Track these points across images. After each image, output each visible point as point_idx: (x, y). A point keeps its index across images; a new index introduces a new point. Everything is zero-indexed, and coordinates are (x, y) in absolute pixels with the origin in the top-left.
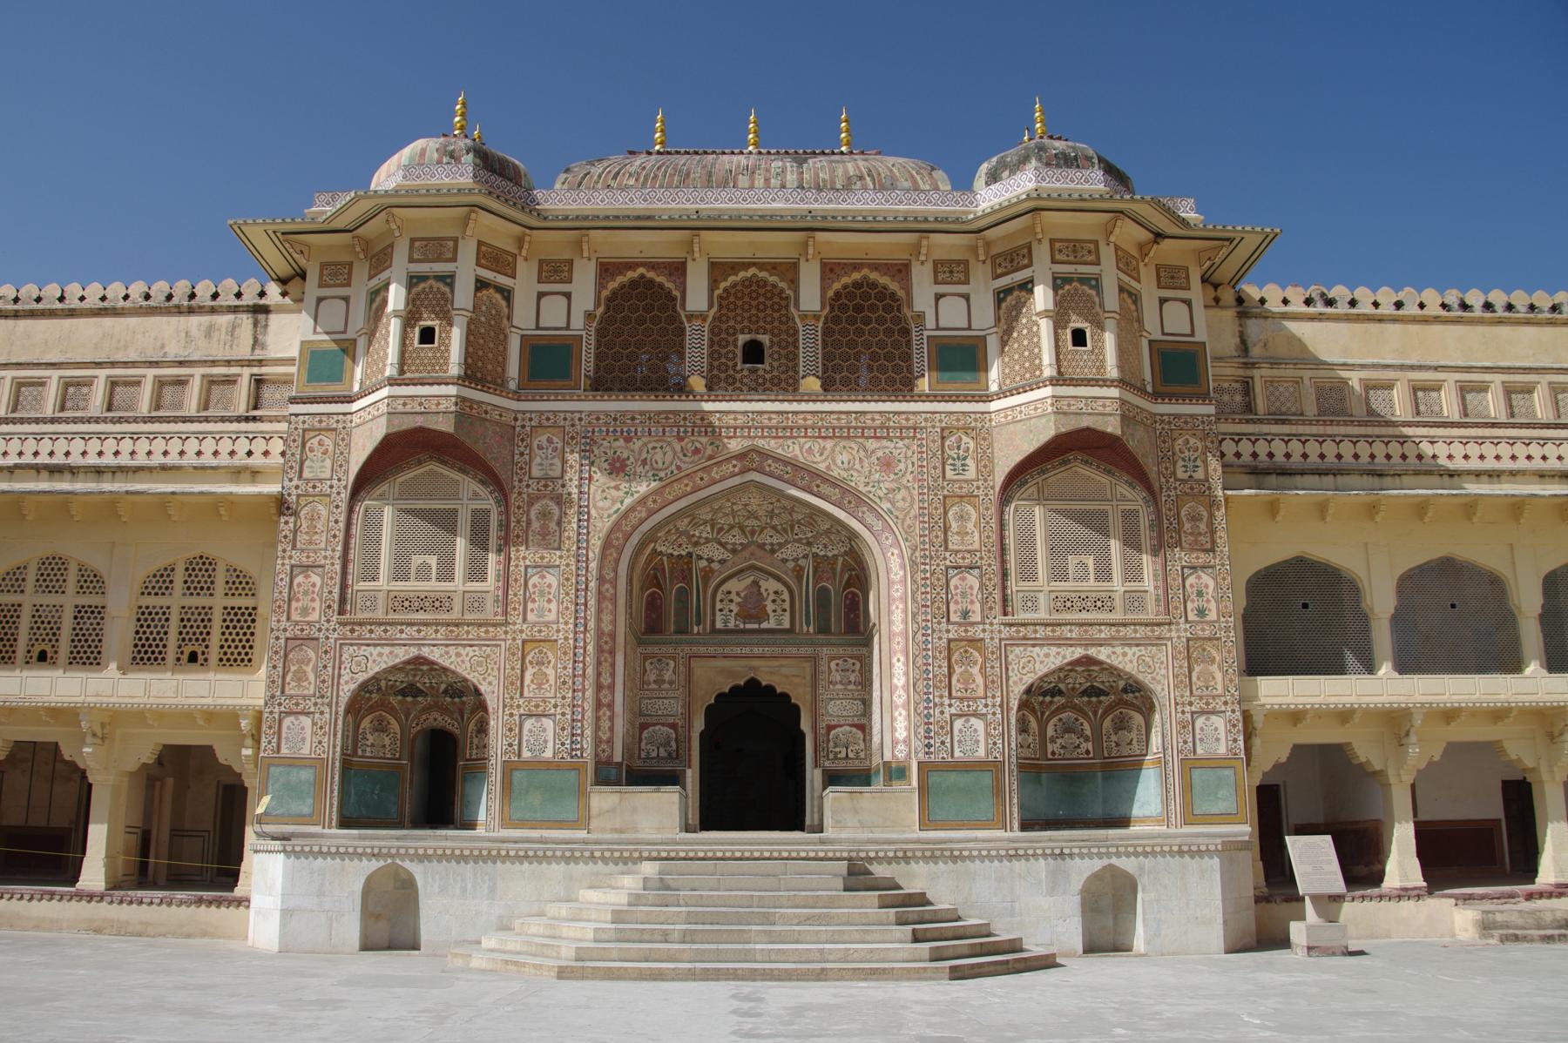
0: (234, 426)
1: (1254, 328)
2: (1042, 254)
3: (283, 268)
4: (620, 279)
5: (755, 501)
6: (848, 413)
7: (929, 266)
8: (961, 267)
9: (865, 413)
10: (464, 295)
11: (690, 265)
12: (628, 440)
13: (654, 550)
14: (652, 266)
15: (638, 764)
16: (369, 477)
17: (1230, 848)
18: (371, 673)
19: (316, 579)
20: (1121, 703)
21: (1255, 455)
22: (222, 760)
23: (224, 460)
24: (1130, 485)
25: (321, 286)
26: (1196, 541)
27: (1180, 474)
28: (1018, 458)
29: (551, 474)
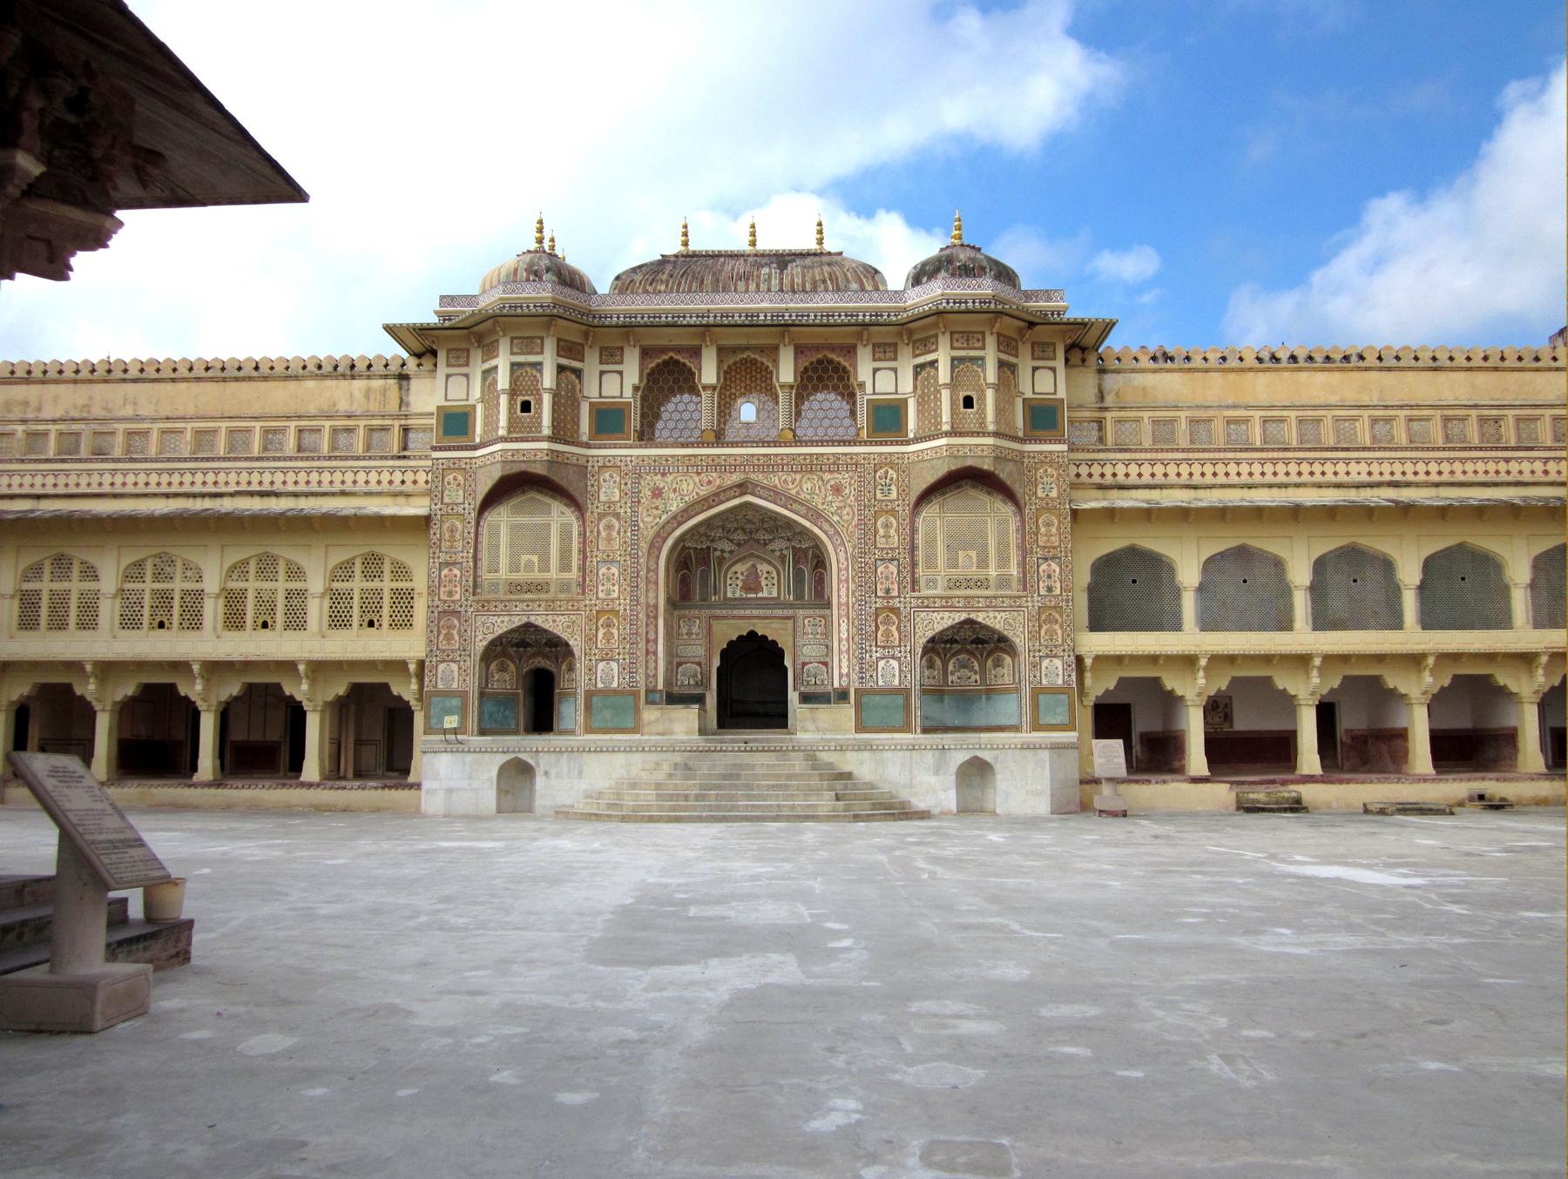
0: (391, 463)
1: (1110, 381)
3: (418, 348)
7: (870, 348)
12: (664, 475)
14: (679, 350)
15: (676, 690)
19: (456, 572)
21: (1102, 475)
23: (385, 486)
27: (1040, 494)
28: (924, 486)
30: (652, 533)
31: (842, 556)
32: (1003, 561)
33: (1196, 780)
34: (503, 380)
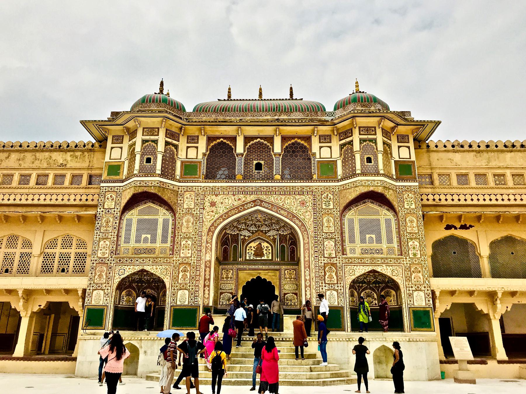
2: (356, 132)
5: (259, 216)
6: (290, 187)
7: (318, 137)
8: (329, 137)
9: (295, 186)
11: (238, 138)
12: (216, 195)
13: (225, 232)
14: (225, 138)
15: (219, 307)
20: (387, 287)
21: (434, 200)
22: (71, 307)
24: (388, 210)
25: (112, 143)
26: (412, 229)
27: (406, 206)
28: (348, 201)
29: (191, 207)
30: (210, 224)
32: (390, 240)
33: (500, 362)
34: (138, 148)
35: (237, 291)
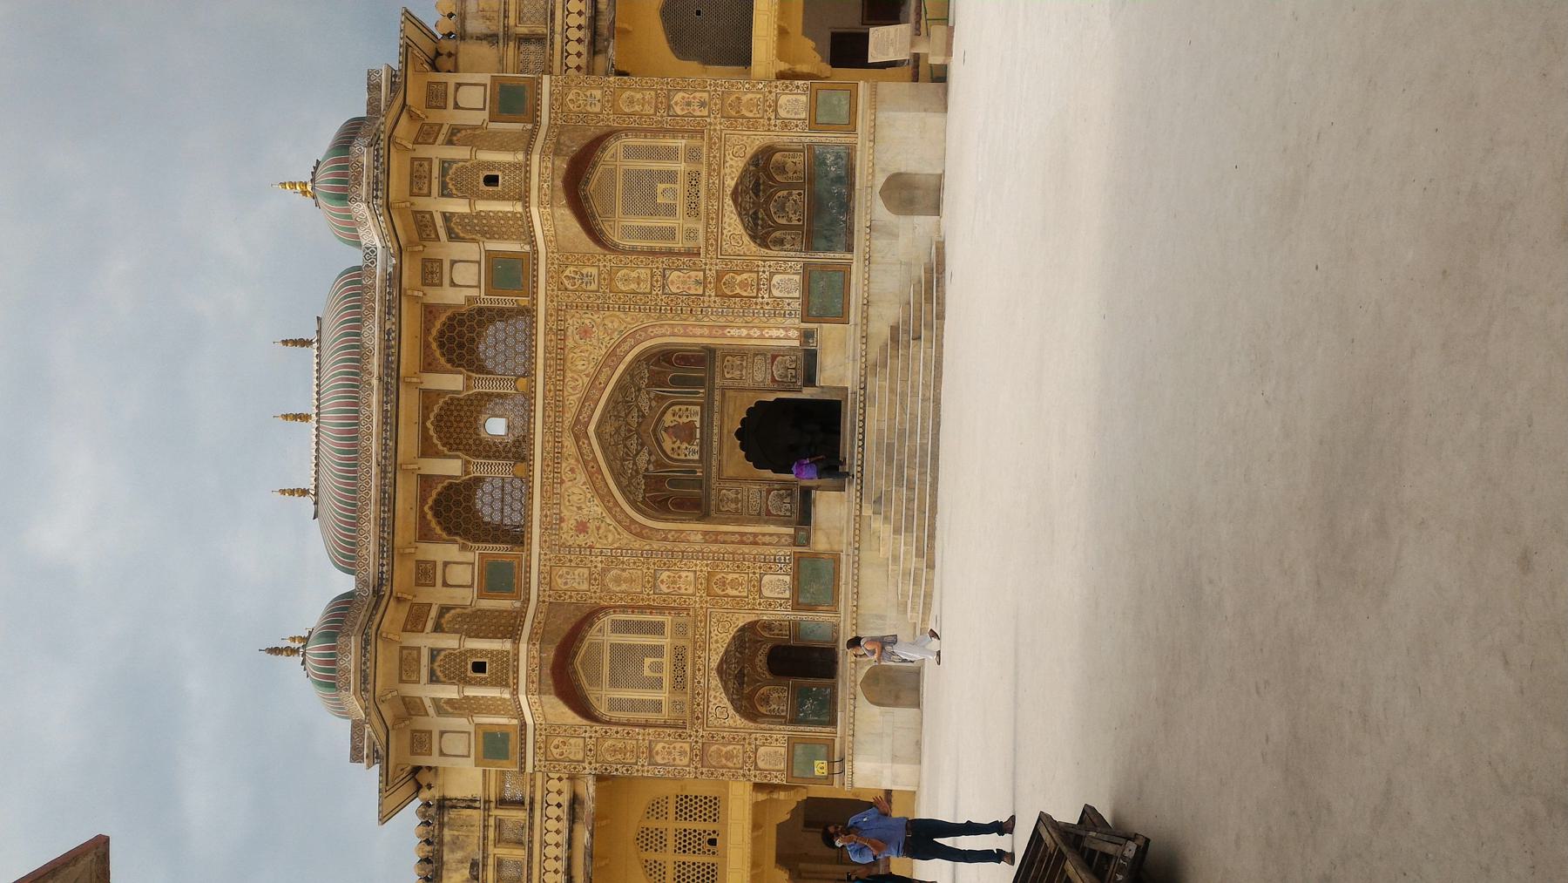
1: (475, 26)
2: (422, 203)
3: (408, 788)
4: (433, 524)
5: (609, 429)
9: (546, 347)
10: (449, 642)
12: (562, 520)
14: (423, 501)
16: (582, 707)
17: (874, 93)
18: (729, 704)
19: (659, 747)
20: (766, 169)
21: (579, 41)
24: (604, 149)
27: (597, 109)
28: (584, 235)
30: (625, 534)
31: (657, 331)
32: (671, 154)
34: (449, 692)
35: (762, 480)
